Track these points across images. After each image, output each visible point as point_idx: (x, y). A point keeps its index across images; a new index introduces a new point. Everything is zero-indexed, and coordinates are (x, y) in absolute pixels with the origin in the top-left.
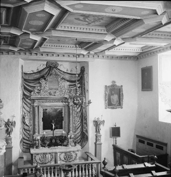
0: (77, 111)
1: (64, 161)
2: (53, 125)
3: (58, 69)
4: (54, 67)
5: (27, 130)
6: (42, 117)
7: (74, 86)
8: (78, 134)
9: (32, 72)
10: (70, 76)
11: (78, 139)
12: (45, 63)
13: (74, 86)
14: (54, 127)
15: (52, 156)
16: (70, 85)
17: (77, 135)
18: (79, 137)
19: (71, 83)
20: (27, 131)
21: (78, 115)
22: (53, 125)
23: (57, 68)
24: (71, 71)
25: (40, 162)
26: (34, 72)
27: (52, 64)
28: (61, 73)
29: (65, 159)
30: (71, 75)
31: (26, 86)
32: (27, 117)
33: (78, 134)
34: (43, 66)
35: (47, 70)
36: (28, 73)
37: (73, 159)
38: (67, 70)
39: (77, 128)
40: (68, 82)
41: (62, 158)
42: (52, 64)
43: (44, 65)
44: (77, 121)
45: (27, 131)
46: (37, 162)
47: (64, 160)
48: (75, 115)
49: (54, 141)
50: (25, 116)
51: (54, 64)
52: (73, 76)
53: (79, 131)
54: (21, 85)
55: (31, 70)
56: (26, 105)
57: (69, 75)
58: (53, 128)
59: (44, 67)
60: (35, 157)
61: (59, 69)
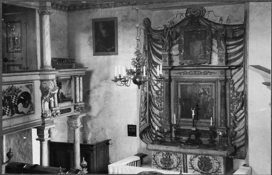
0: (239, 90)
1: (198, 171)
2: (193, 111)
3: (205, 19)
4: (199, 17)
5: (157, 116)
8: (240, 130)
12: (184, 11)
13: (233, 47)
14: (193, 114)
15: (179, 159)
18: (242, 136)
20: (158, 118)
21: (239, 97)
22: (193, 111)
23: (203, 17)
25: (161, 165)
27: (195, 12)
29: (200, 168)
31: (156, 49)
33: (240, 130)
34: (182, 17)
35: (188, 22)
36: (159, 29)
37: (214, 171)
38: (221, 19)
39: (238, 120)
41: (194, 166)
42: (195, 12)
43: (182, 14)
44: (238, 108)
45: (158, 118)
46: (157, 164)
47: (199, 169)
48: (233, 98)
49: (193, 137)
51: (199, 11)
53: (243, 126)
54: (144, 48)
58: (193, 117)
59: (183, 18)
60: (154, 156)
61: (207, 20)
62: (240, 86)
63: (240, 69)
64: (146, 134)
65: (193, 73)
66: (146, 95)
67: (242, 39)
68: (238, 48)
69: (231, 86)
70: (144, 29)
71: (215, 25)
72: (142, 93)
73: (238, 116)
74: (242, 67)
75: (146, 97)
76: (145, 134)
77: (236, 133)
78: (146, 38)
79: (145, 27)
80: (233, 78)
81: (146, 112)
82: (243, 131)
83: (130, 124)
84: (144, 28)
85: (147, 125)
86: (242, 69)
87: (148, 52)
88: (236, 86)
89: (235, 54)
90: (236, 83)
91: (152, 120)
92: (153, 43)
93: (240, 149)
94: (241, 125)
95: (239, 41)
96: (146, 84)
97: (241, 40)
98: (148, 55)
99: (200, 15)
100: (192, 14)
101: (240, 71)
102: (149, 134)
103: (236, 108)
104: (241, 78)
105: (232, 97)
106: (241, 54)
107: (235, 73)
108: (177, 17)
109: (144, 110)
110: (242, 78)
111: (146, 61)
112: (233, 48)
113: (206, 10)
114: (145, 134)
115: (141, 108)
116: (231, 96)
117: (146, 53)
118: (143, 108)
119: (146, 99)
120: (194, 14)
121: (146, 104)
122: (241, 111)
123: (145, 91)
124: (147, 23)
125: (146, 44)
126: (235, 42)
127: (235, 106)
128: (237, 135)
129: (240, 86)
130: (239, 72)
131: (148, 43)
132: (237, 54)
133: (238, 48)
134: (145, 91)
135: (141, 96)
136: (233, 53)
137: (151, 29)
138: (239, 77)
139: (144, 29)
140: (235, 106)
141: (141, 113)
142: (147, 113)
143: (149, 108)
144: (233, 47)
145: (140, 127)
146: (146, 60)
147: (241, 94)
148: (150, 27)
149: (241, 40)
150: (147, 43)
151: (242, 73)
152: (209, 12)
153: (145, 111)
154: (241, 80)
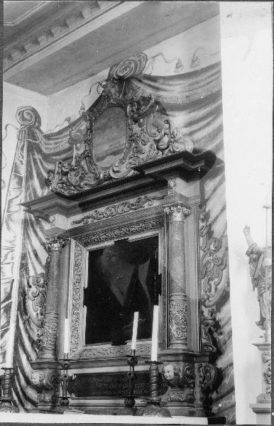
6: (85, 283)
7: (205, 122)
9: (66, 124)
10: (191, 85)
13: (211, 118)
16: (190, 124)
24: (193, 61)
26: (72, 120)
32: (34, 289)
38: (178, 65)
40: (184, 113)
42: (125, 69)
48: (208, 258)
50: (30, 287)
51: (133, 65)
57: (187, 82)
61: (150, 78)
65: (113, 210)
66: (10, 285)
69: (201, 224)
71: (167, 83)
75: (8, 290)
78: (22, 149)
79: (22, 125)
81: (6, 331)
84: (19, 126)
87: (27, 181)
90: (217, 217)
91: (23, 358)
92: (43, 161)
98: (27, 189)
99: (135, 71)
100: (121, 75)
103: (216, 289)
105: (204, 256)
112: (208, 124)
113: (149, 57)
116: (202, 253)
117: (20, 183)
120: (125, 73)
124: (31, 122)
125: (21, 162)
127: (212, 283)
131: (28, 162)
137: (41, 132)
140: (212, 283)
148: (38, 128)
150: (25, 162)
152: (154, 57)
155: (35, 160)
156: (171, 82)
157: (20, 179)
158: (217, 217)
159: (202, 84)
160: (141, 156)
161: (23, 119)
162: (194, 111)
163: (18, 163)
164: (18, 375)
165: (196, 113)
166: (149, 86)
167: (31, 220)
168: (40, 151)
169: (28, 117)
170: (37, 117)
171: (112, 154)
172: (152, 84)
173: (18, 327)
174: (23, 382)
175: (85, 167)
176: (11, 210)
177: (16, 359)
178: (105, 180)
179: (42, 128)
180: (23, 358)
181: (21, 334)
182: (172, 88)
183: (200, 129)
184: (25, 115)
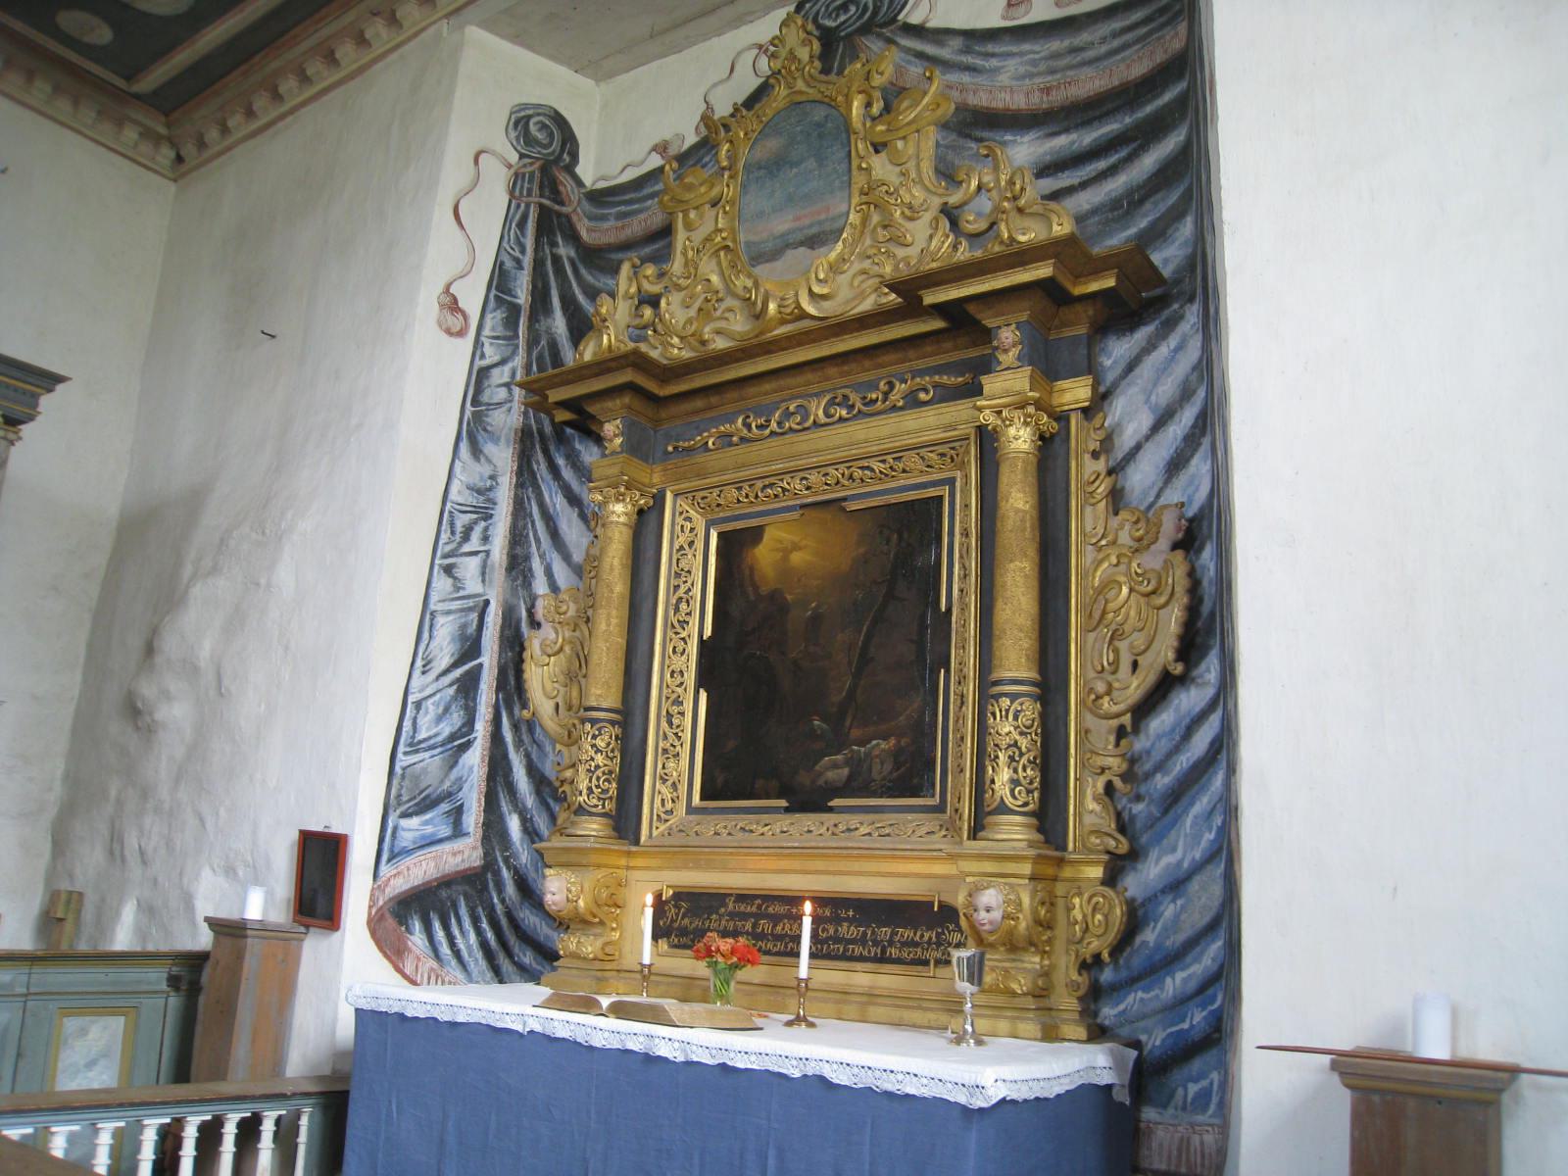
6: (701, 623)
7: (1102, 164)
8: (1176, 885)
9: (656, 161)
11: (1174, 983)
13: (1113, 159)
16: (1044, 170)
17: (1169, 910)
19: (1062, 140)
23: (894, 20)
28: (944, 53)
30: (1056, 45)
32: (548, 632)
39: (1162, 782)
50: (535, 624)
52: (1084, 37)
54: (500, 281)
55: (656, 140)
56: (574, 514)
61: (918, 31)
62: (1176, 465)
63: (1170, 325)
64: (446, 927)
66: (474, 616)
67: (1179, 87)
68: (1149, 161)
70: (509, 166)
72: (434, 597)
73: (1164, 746)
74: (1191, 299)
75: (472, 629)
76: (437, 925)
77: (1135, 919)
78: (522, 225)
79: (522, 156)
80: (1118, 407)
82: (1205, 894)
83: (316, 826)
84: (514, 157)
85: (465, 854)
86: (1192, 314)
87: (533, 318)
88: (1142, 476)
89: (1127, 213)
90: (1138, 447)
91: (514, 824)
92: (583, 271)
93: (1176, 1075)
94: (1196, 838)
95: (1149, 109)
96: (485, 539)
97: (1168, 97)
98: (533, 341)
99: (875, 13)
100: (830, 23)
101: (1173, 341)
102: (479, 932)
103: (1135, 665)
104: (1185, 394)
106: (1174, 197)
107: (1131, 367)
108: (735, 74)
109: (446, 729)
110: (1194, 392)
111: (500, 375)
112: (1112, 171)
114: (437, 925)
115: (418, 705)
117: (511, 321)
118: (431, 709)
119: (470, 648)
120: (842, 18)
121: (468, 687)
122: (1188, 700)
123: (473, 586)
125: (518, 261)
126: (1128, 120)
127: (1123, 645)
128: (1149, 936)
129: (1176, 465)
130: (1164, 350)
131: (538, 265)
132: (1148, 206)
133: (1149, 161)
134: (473, 586)
135: (427, 619)
136: (1114, 204)
137: (579, 183)
138: (1167, 390)
139: (509, 166)
140: (1123, 645)
141: (401, 748)
142: (475, 759)
143: (496, 721)
144: (1113, 159)
145: (388, 850)
146: (507, 368)
147: (1169, 528)
148: (570, 170)
149: (1168, 97)
150: (528, 260)
151: (1193, 353)
153: (452, 737)
154: (1188, 416)
155: (557, 260)
156: (990, 48)
157: (514, 311)
158: (1138, 447)
159: (1090, 54)
160: (901, 252)
161: (528, 139)
162: (1067, 130)
163: (509, 264)
164: (497, 874)
165: (1073, 136)
166: (921, 56)
167: (541, 432)
168: (573, 237)
169: (540, 136)
170: (569, 141)
171: (802, 244)
172: (930, 49)
173: (496, 737)
174: (510, 889)
175: (715, 279)
176: (485, 398)
177: (493, 827)
178: (783, 322)
179: (579, 170)
180: (514, 824)
181: (505, 756)
182: (994, 62)
183: (1084, 185)
184: (533, 128)
